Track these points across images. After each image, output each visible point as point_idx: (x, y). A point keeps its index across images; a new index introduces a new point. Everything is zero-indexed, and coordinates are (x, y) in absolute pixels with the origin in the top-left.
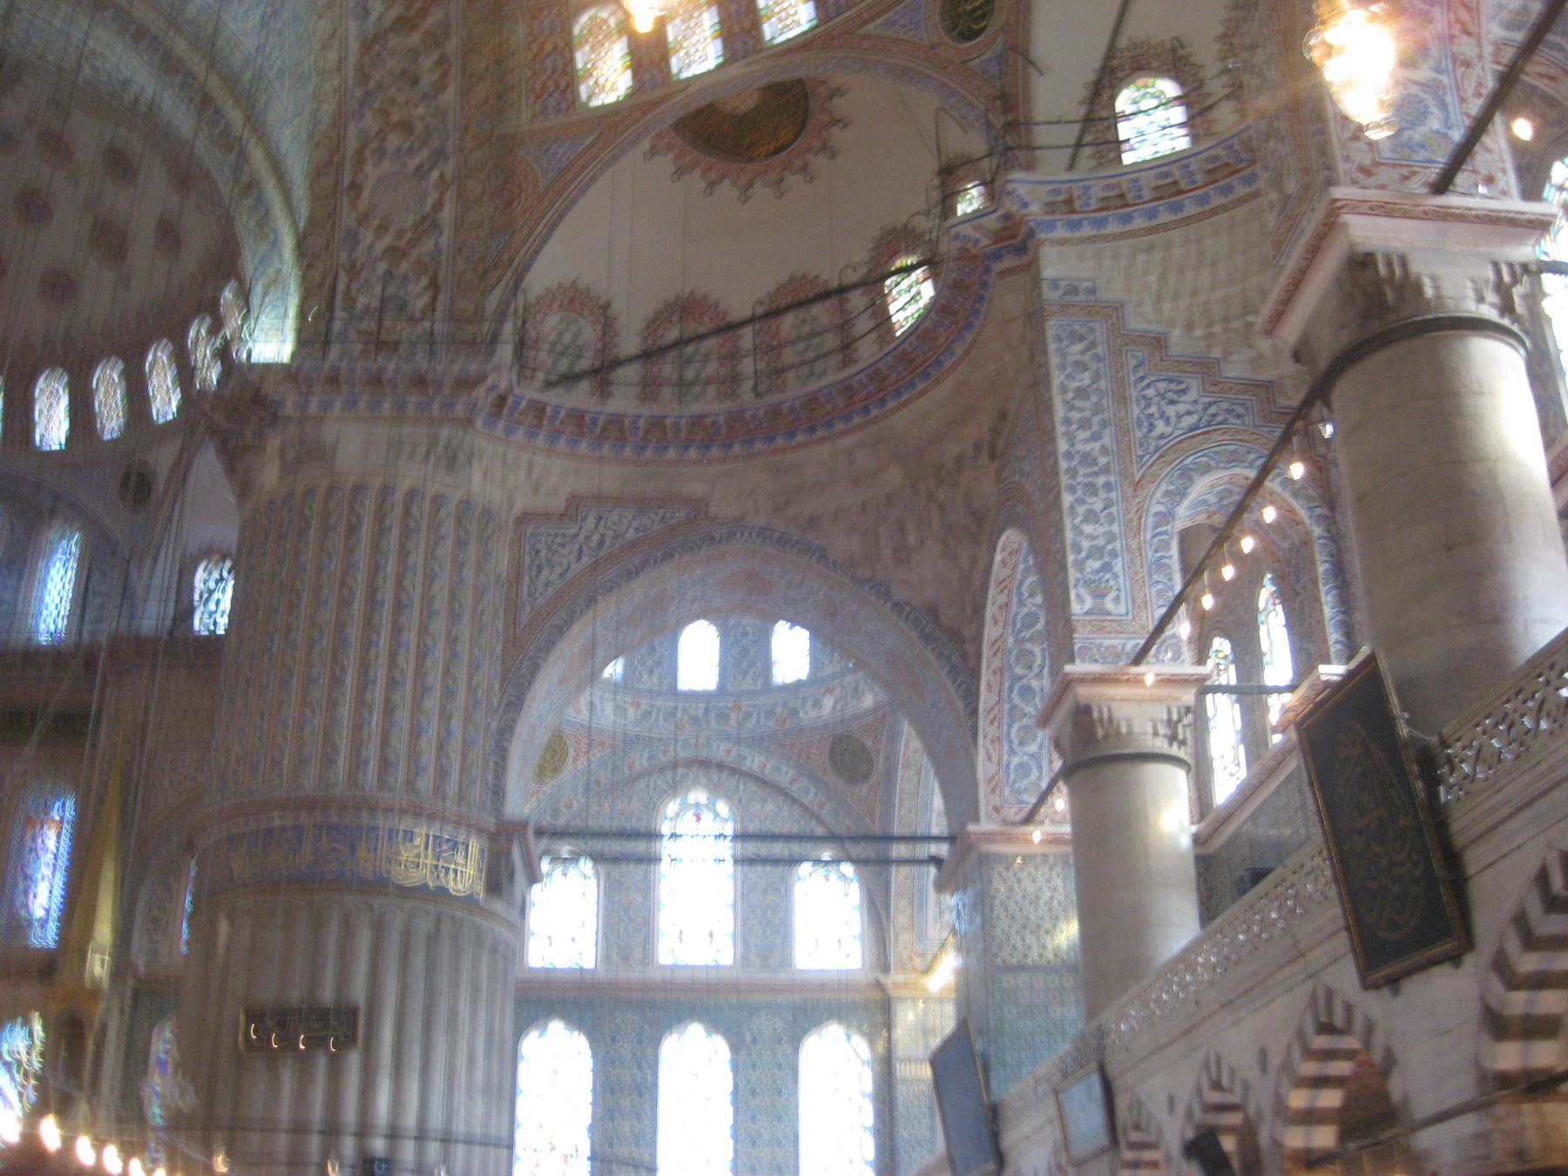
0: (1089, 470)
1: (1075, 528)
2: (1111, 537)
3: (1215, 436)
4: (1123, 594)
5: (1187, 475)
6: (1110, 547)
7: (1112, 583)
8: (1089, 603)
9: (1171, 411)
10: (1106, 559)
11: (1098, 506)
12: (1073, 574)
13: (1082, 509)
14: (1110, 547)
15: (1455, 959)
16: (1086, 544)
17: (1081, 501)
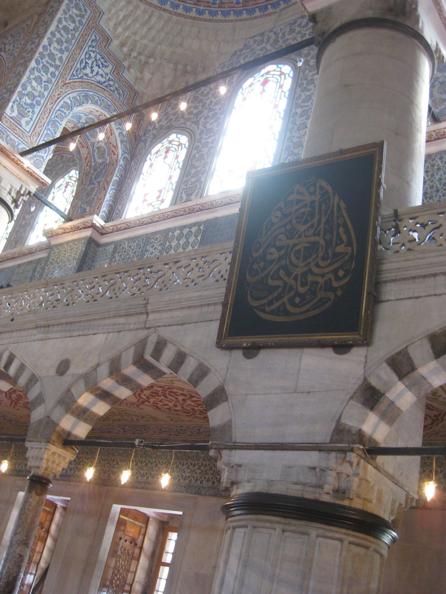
0: (50, 61)
1: (29, 78)
2: (41, 95)
3: (106, 93)
4: (32, 123)
5: (87, 98)
6: (39, 99)
7: (30, 114)
8: (15, 114)
9: (96, 69)
10: (34, 103)
11: (44, 78)
12: (15, 96)
13: (36, 74)
14: (39, 99)
15: (342, 348)
16: (29, 89)
17: (39, 71)
